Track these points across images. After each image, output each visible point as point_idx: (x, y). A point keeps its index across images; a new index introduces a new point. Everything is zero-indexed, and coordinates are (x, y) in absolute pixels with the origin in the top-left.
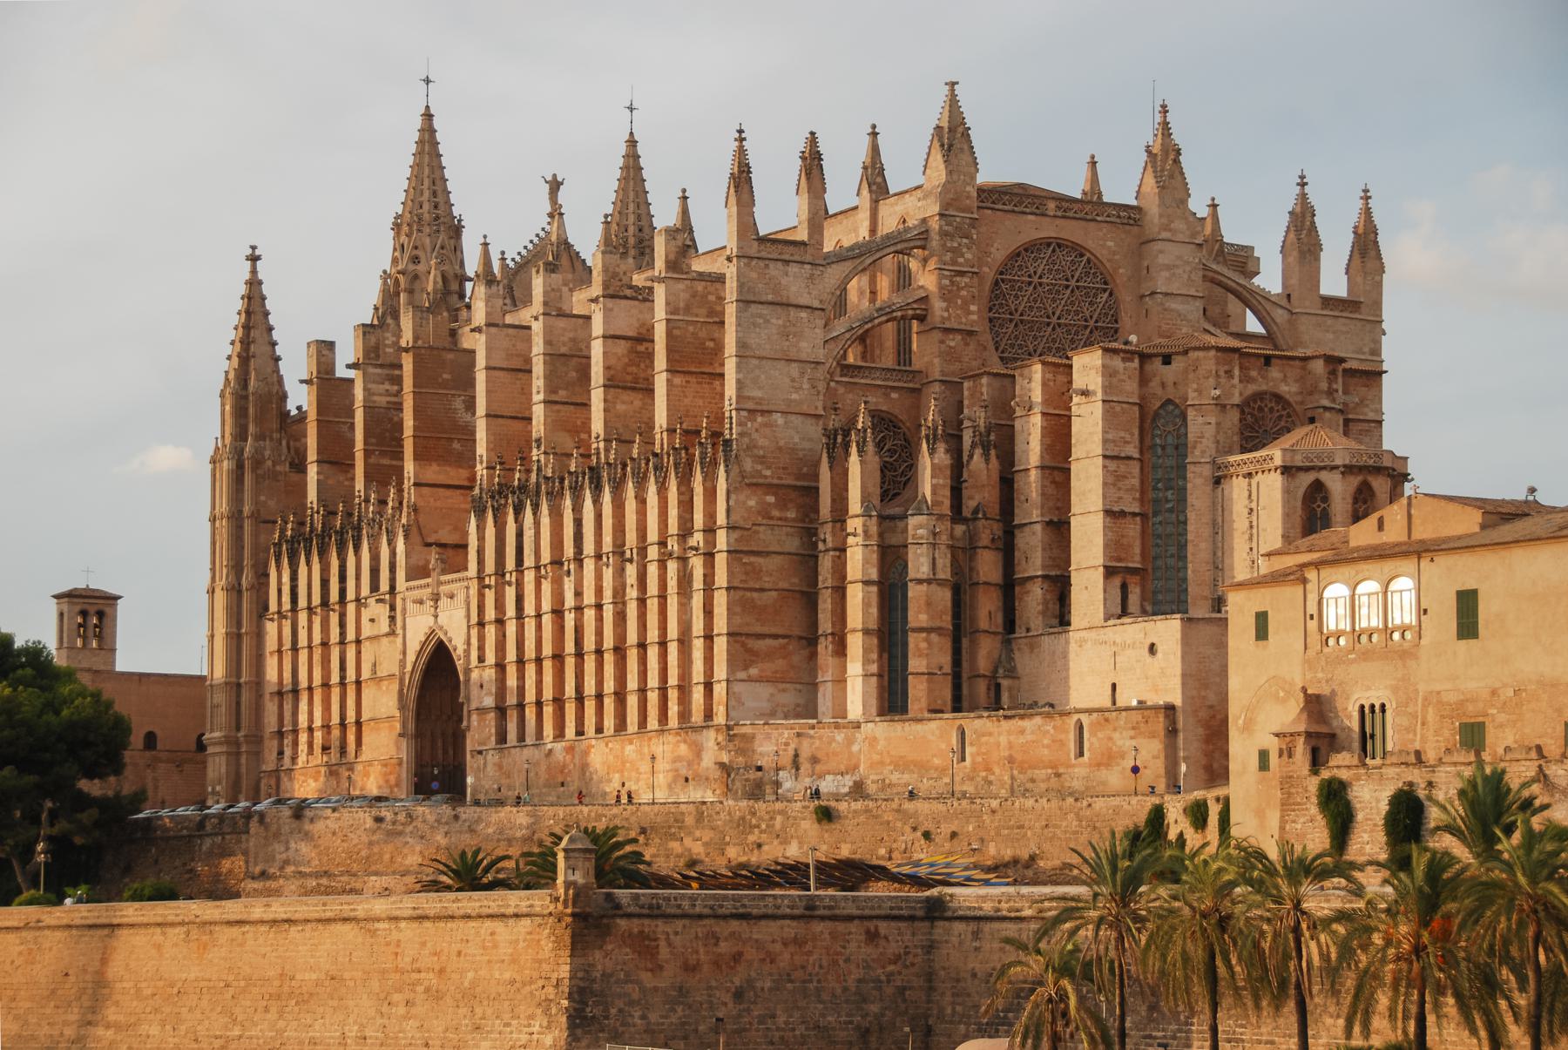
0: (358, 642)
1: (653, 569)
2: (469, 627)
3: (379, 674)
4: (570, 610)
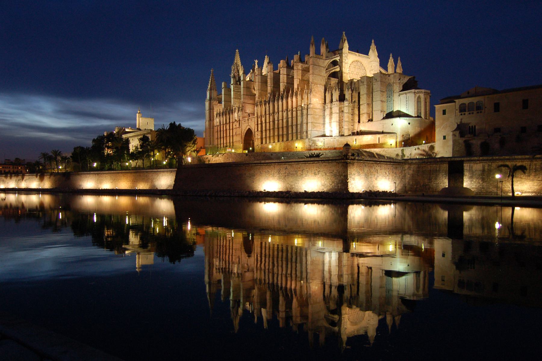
0: (233, 129)
1: (294, 113)
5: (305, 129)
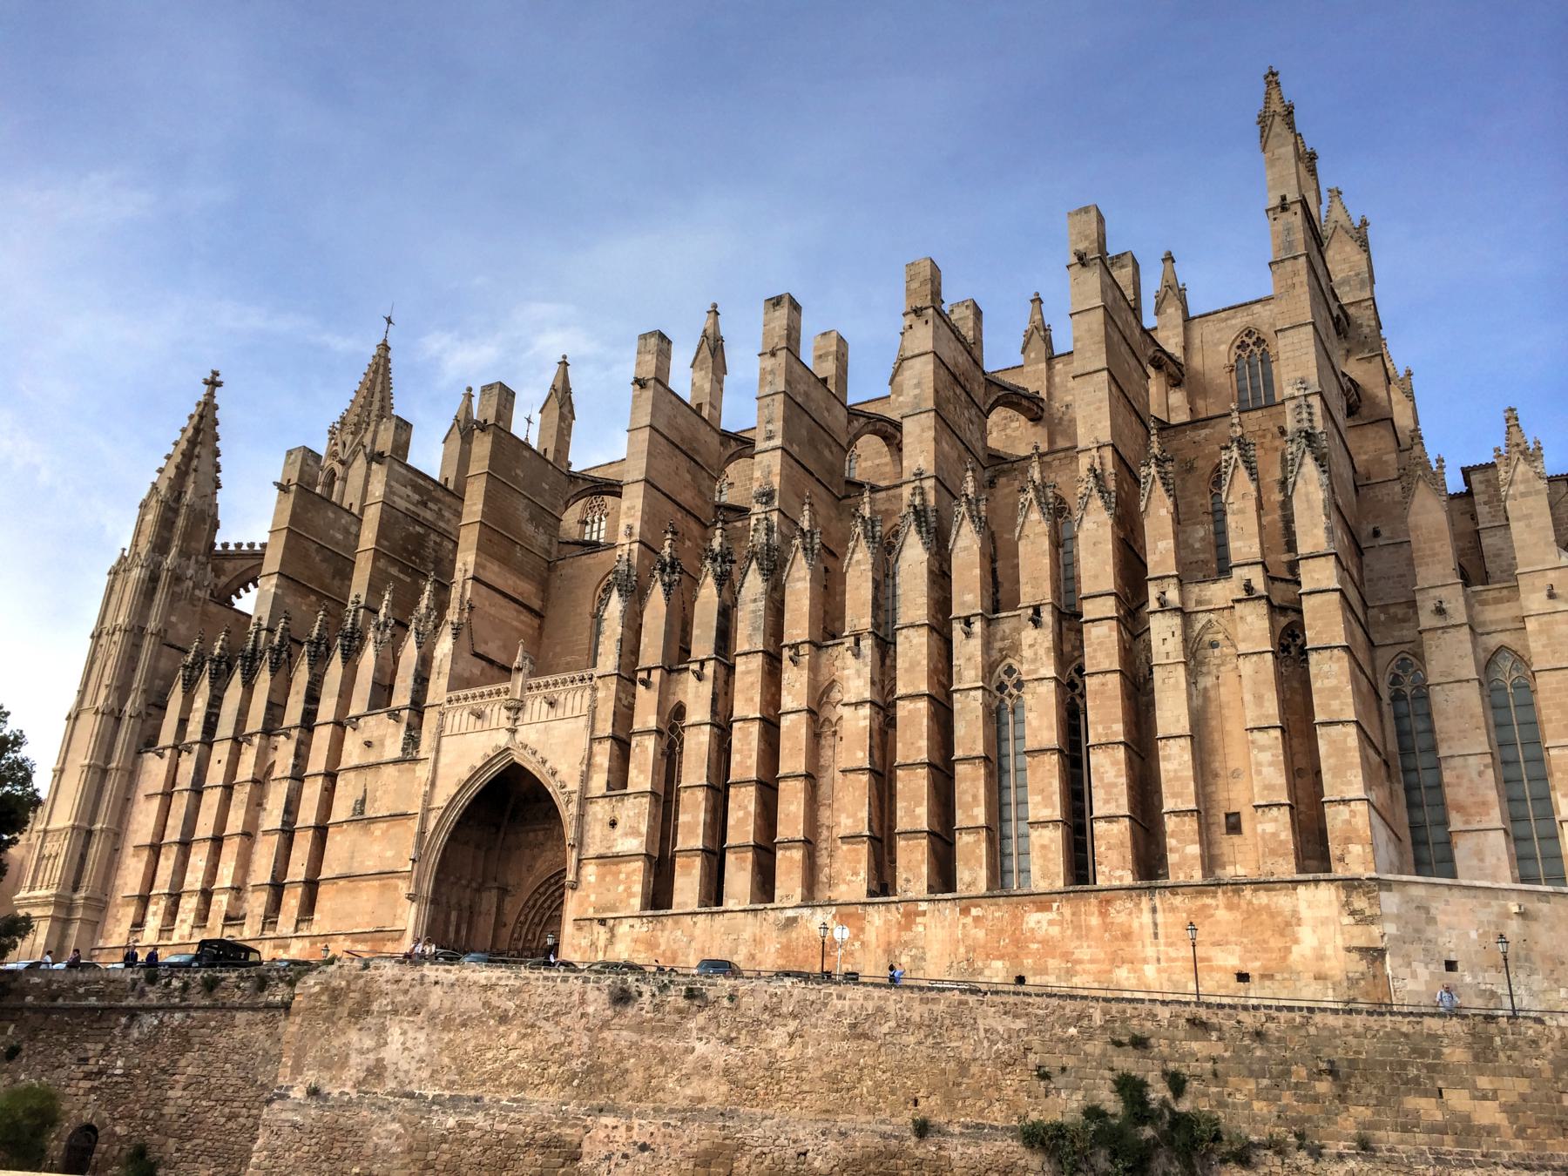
0: (331, 777)
2: (592, 740)
3: (369, 812)
4: (857, 705)
5: (1269, 787)
